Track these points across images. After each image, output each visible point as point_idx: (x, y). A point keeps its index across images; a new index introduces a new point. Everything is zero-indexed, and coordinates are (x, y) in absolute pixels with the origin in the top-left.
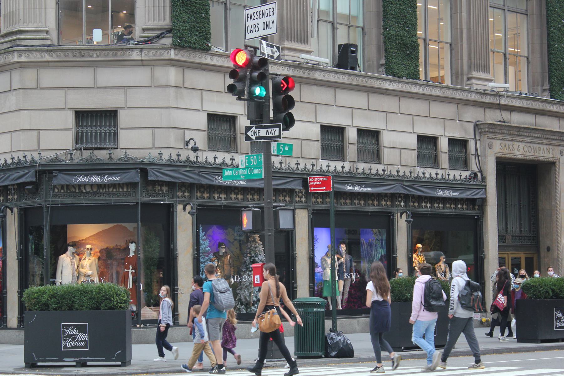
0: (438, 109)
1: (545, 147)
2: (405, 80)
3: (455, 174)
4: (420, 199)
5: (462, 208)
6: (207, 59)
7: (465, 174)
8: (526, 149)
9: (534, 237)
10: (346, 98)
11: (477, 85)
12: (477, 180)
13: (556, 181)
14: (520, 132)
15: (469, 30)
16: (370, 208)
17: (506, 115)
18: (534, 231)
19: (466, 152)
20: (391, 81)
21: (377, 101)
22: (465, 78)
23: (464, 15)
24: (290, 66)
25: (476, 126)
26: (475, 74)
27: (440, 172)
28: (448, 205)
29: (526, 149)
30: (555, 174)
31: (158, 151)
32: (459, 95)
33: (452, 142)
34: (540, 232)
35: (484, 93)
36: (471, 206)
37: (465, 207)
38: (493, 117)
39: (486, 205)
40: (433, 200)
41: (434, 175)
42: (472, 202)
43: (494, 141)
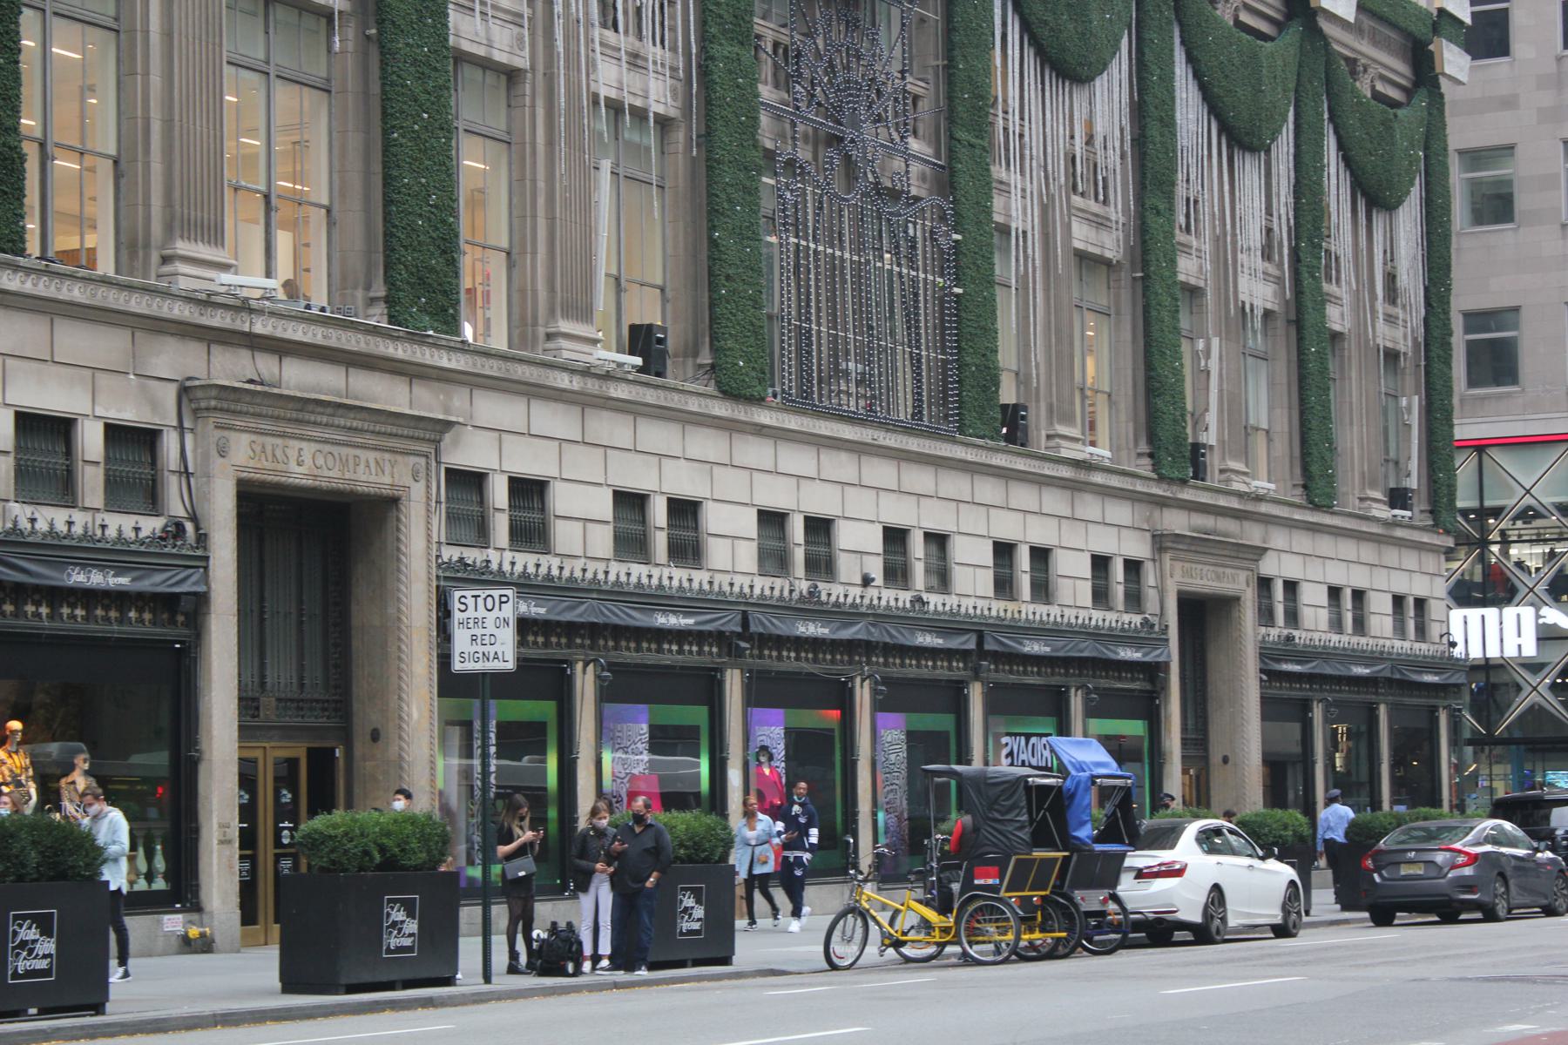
0: (76, 341)
3: (120, 525)
5: (141, 621)
7: (151, 525)
8: (320, 461)
9: (336, 702)
11: (188, 279)
12: (183, 543)
13: (398, 549)
14: (303, 412)
15: (168, 123)
17: (266, 365)
18: (336, 687)
19: (154, 463)
22: (155, 258)
23: (156, 80)
25: (185, 391)
26: (182, 247)
27: (80, 518)
28: (99, 612)
29: (320, 461)
30: (398, 530)
32: (137, 304)
33: (116, 433)
34: (354, 689)
35: (207, 302)
36: (165, 616)
37: (147, 616)
38: (231, 368)
39: (208, 613)
40: (58, 596)
41: (61, 527)
42: (167, 603)
43: (233, 435)
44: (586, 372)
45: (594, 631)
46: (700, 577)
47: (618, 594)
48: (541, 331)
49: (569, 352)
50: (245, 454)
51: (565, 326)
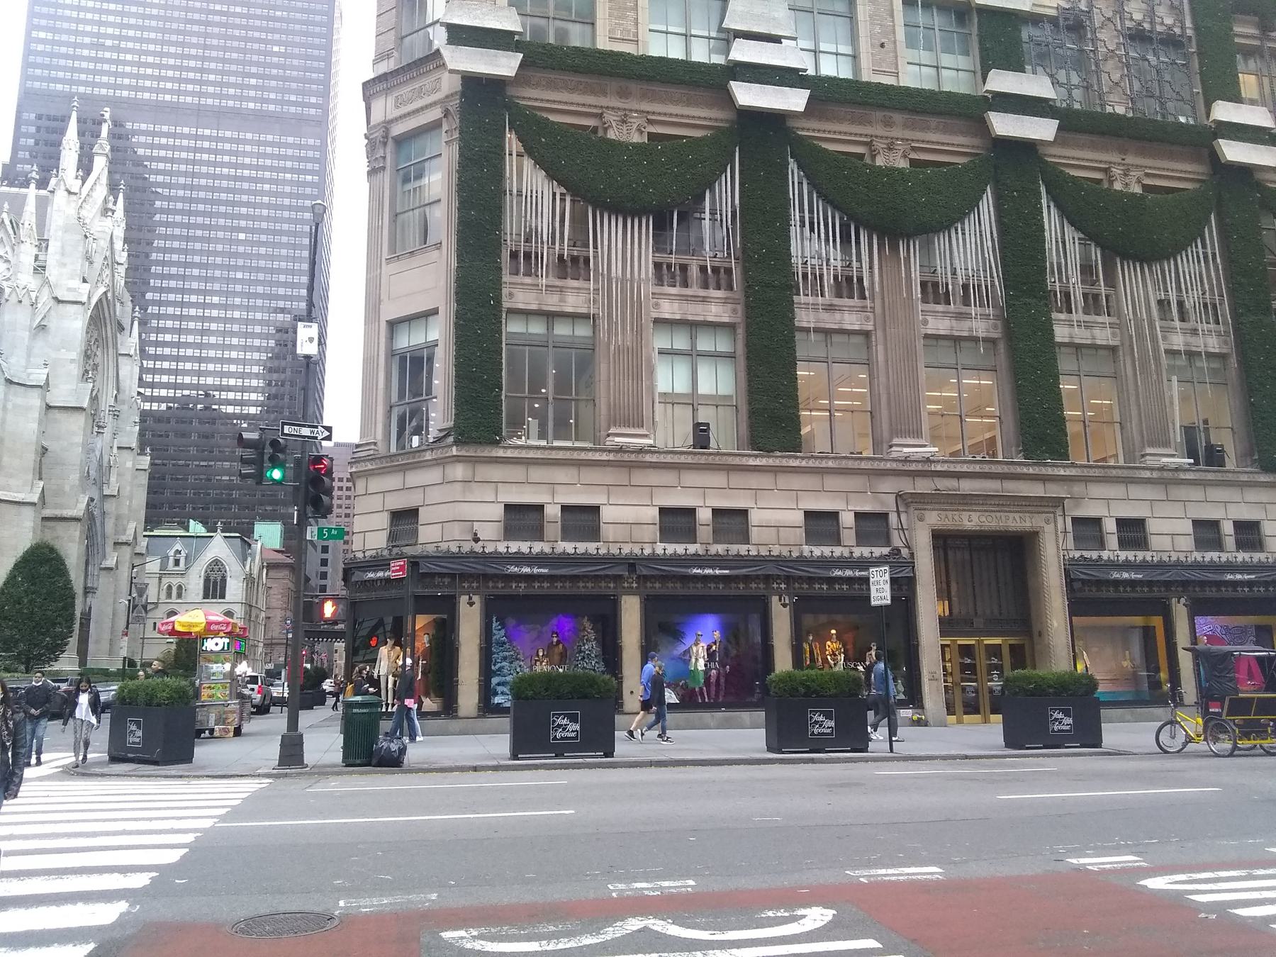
0: (832, 482)
1: (1017, 516)
2: (778, 454)
4: (811, 580)
6: (501, 453)
7: (886, 551)
10: (691, 478)
14: (967, 501)
16: (733, 592)
20: (756, 456)
21: (737, 479)
22: (885, 446)
24: (610, 451)
25: (899, 496)
31: (457, 544)
35: (906, 460)
38: (924, 486)
40: (832, 581)
43: (927, 513)
44: (1162, 469)
45: (1185, 584)
46: (1258, 557)
47: (1197, 566)
48: (1138, 454)
49: (1150, 461)
50: (934, 519)
51: (1149, 450)
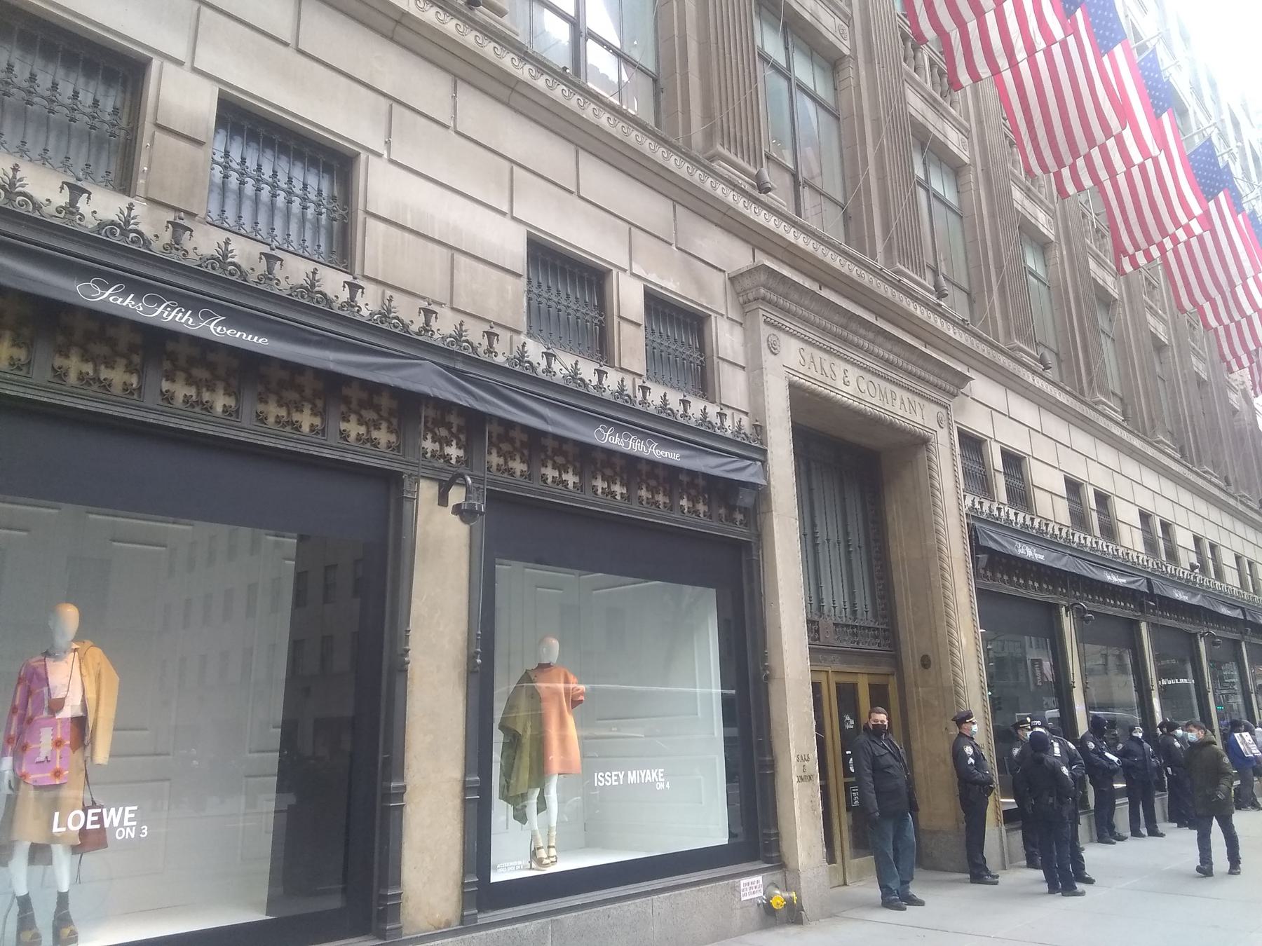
9: (885, 630)
13: (932, 486)
18: (884, 617)
19: (702, 349)
28: (644, 493)
29: (863, 387)
30: (930, 468)
33: (657, 304)
34: (899, 617)
36: (722, 511)
39: (770, 511)
